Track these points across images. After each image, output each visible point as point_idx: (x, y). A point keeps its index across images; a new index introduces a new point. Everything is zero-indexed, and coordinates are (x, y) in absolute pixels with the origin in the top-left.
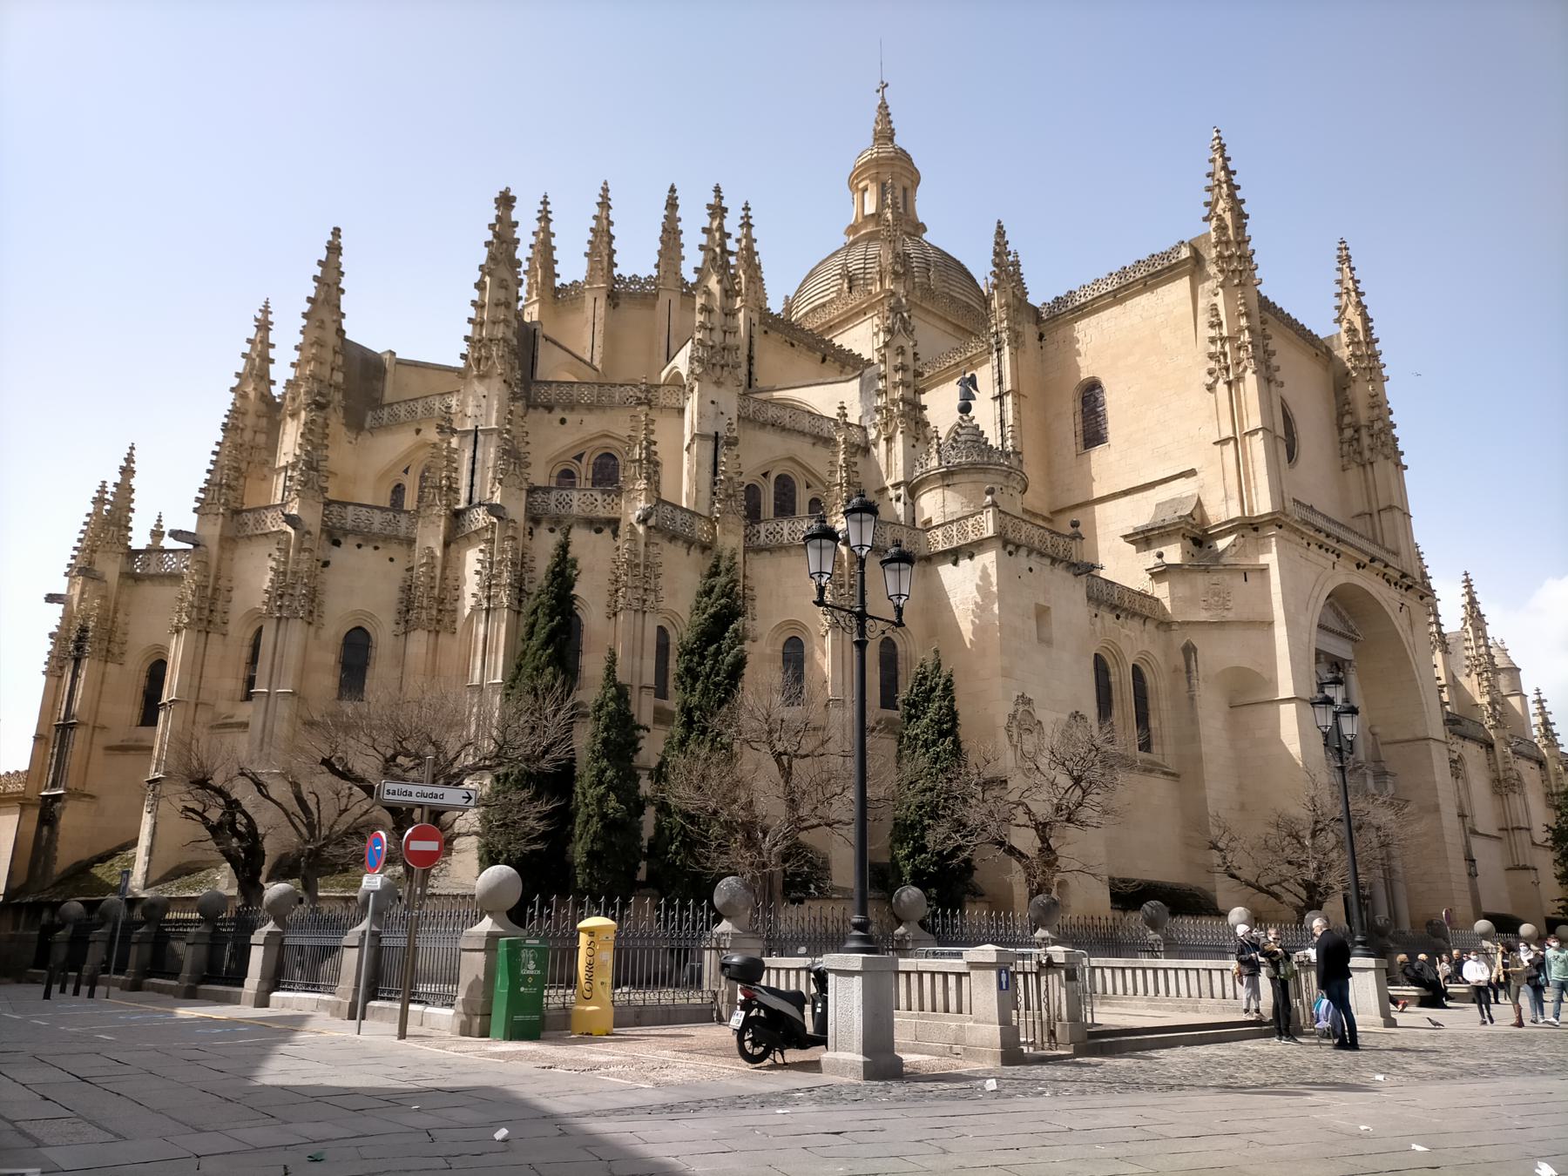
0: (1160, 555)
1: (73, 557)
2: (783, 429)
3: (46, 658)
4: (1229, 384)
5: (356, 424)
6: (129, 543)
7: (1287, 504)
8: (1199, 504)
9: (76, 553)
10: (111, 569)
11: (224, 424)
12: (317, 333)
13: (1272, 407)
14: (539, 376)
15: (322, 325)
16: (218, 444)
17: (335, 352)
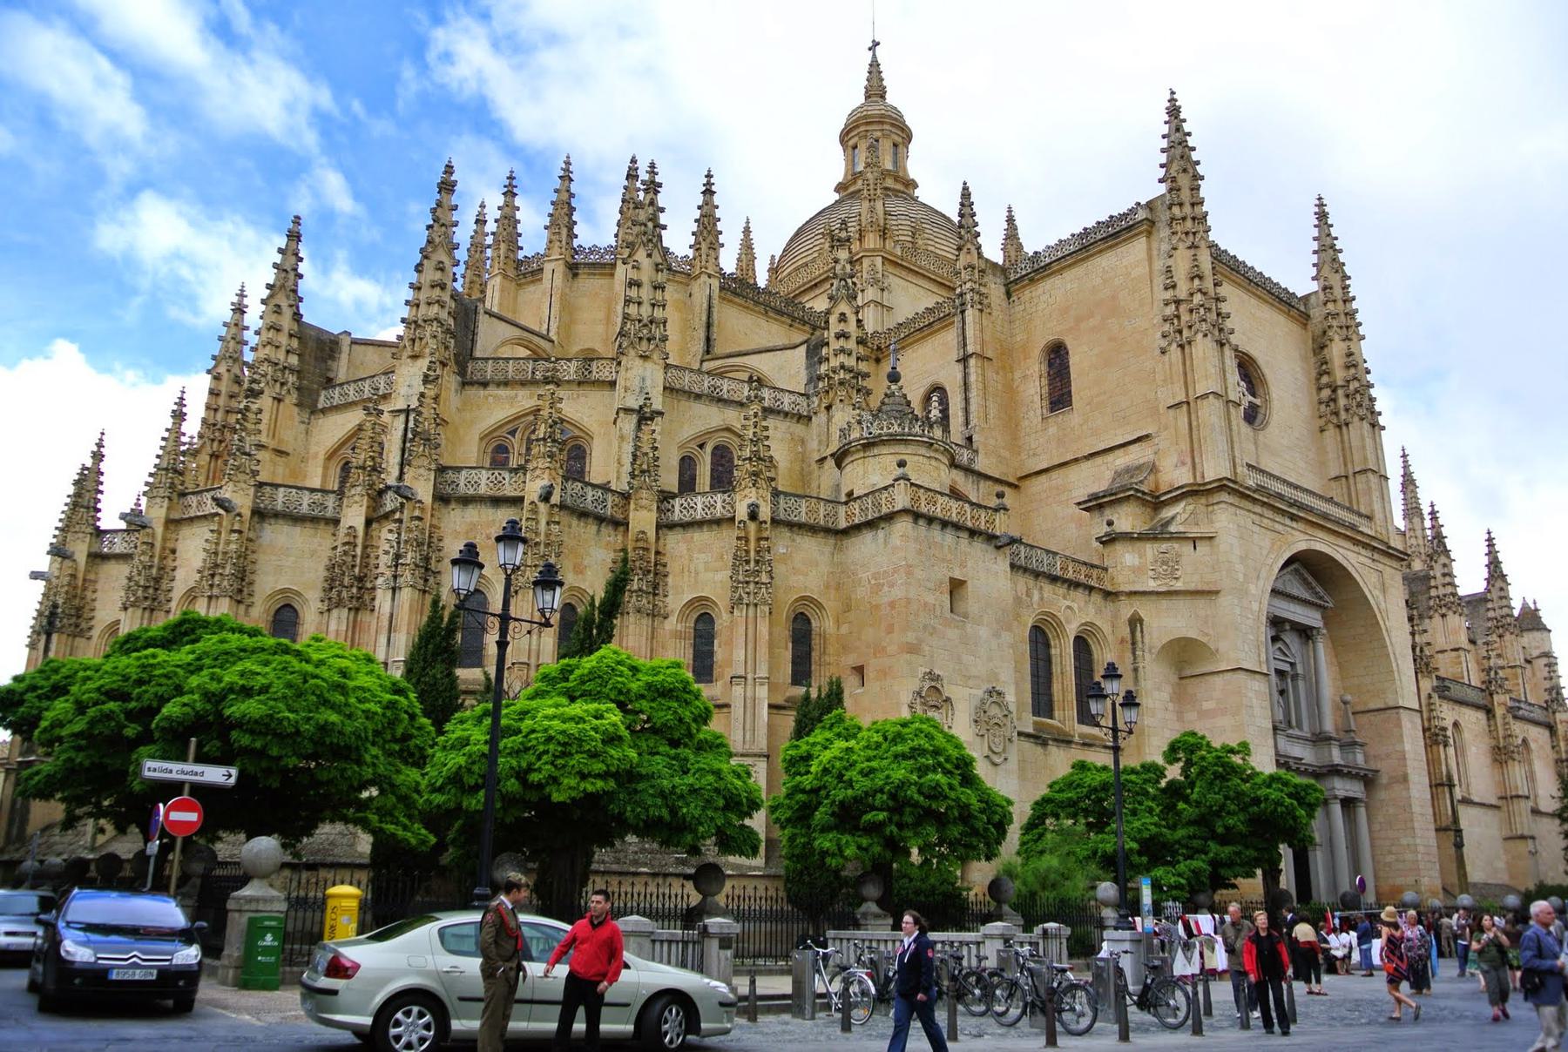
0: (1110, 523)
1: (55, 536)
2: (720, 400)
3: (29, 631)
4: (1181, 346)
5: (310, 406)
6: (98, 524)
7: (1239, 470)
8: (1153, 469)
9: (57, 533)
10: (80, 550)
11: (173, 411)
12: (274, 318)
13: (1224, 371)
14: (478, 354)
15: (278, 310)
16: (167, 430)
17: (291, 336)
